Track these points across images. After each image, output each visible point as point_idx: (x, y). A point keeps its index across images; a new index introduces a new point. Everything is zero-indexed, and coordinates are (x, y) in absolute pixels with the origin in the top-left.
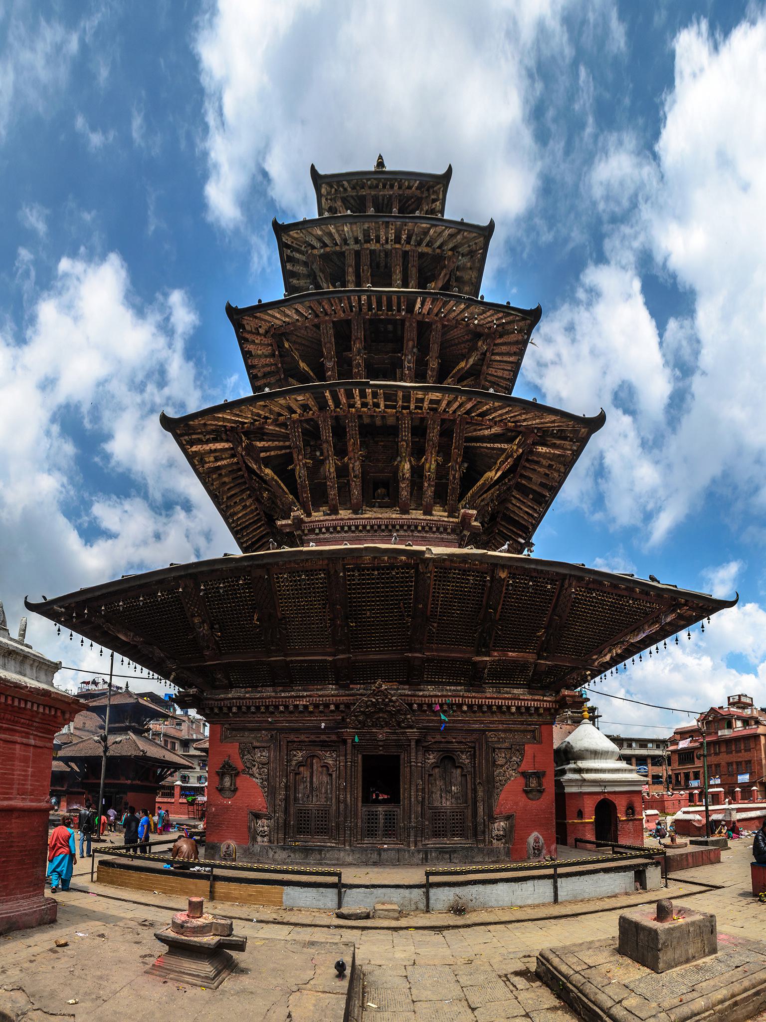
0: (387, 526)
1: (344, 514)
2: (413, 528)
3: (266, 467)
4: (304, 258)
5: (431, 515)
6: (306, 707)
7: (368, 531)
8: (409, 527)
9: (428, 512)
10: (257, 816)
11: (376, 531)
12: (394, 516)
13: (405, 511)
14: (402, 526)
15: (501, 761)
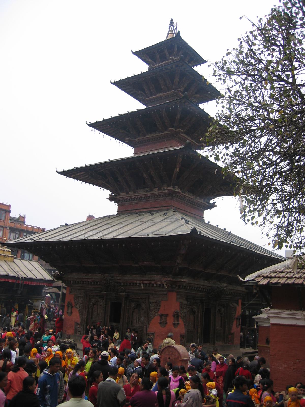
7: (139, 200)
9: (160, 189)
10: (78, 324)
13: (151, 190)
14: (149, 197)
15: (152, 308)
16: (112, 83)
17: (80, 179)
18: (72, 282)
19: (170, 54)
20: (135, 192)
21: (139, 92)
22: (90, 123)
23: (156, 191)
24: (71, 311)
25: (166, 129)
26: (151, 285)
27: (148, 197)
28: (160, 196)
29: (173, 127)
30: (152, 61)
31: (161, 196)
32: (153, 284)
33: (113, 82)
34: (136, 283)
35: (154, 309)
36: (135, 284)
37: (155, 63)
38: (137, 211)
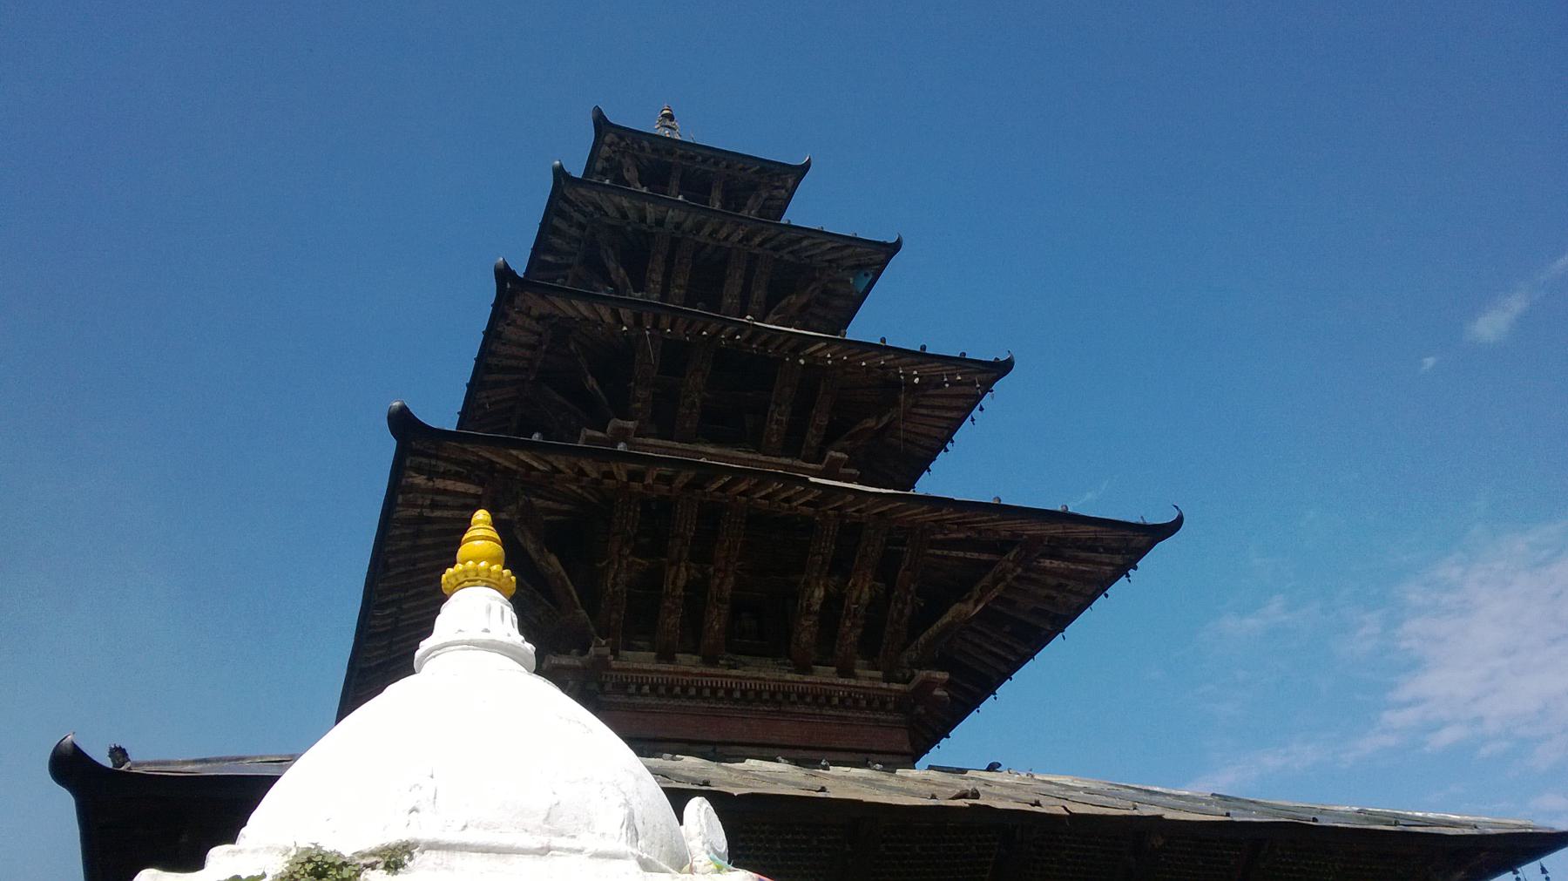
0: (773, 694)
1: (687, 663)
2: (822, 700)
3: (550, 551)
4: (582, 219)
5: (855, 677)
7: (737, 701)
8: (816, 697)
9: (846, 671)
12: (789, 677)
14: (802, 696)
21: (622, 271)
28: (856, 701)
31: (864, 703)
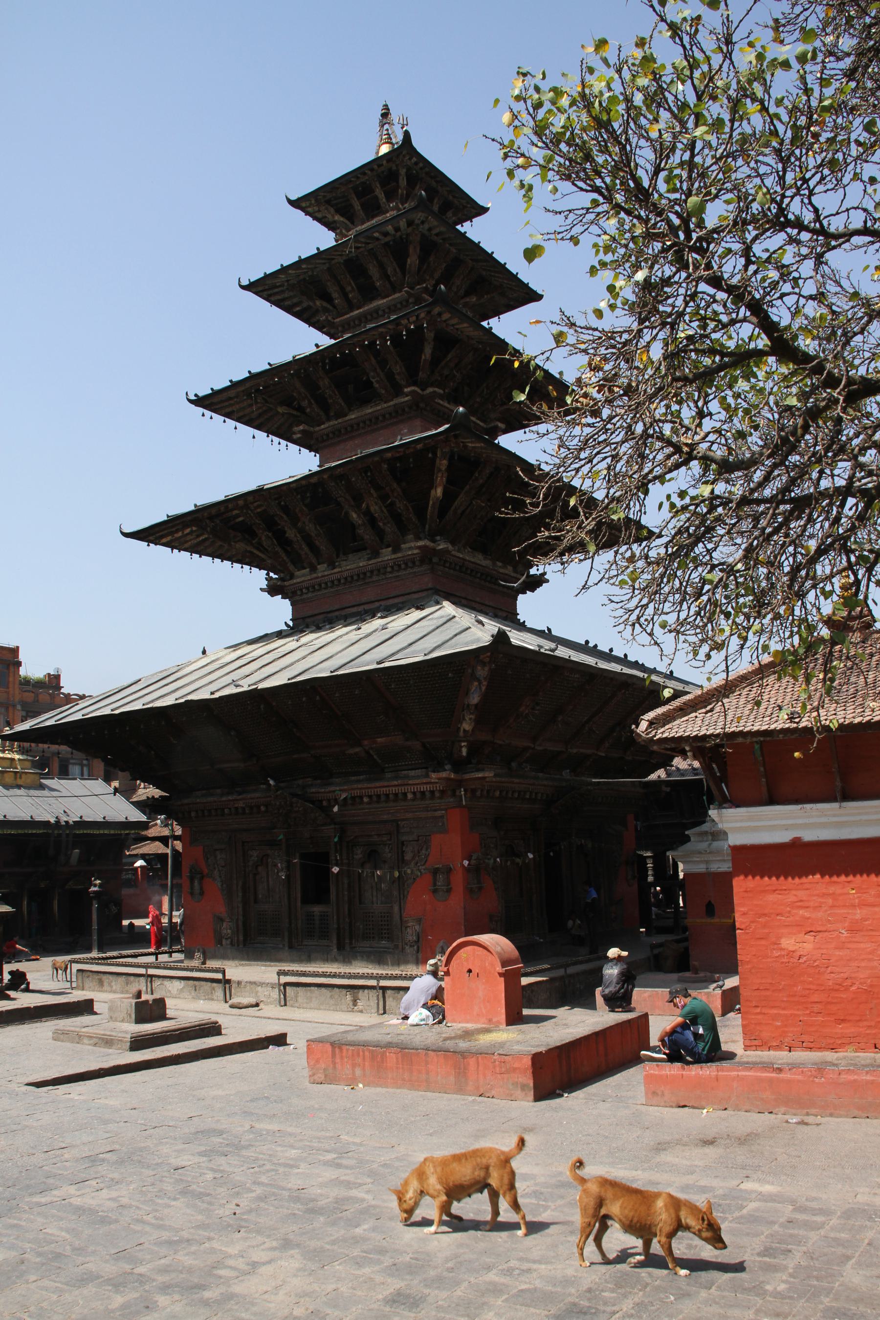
0: (358, 575)
1: (322, 569)
6: (244, 809)
7: (344, 584)
8: (379, 570)
9: (396, 549)
11: (351, 582)
13: (376, 554)
14: (372, 572)
16: (243, 288)
17: (187, 545)
18: (193, 814)
19: (390, 196)
20: (332, 565)
21: (318, 303)
22: (196, 395)
23: (387, 555)
24: (201, 888)
25: (398, 391)
26: (400, 796)
27: (368, 574)
28: (399, 566)
29: (415, 384)
30: (342, 219)
31: (403, 566)
32: (405, 794)
33: (245, 283)
34: (361, 797)
35: (413, 858)
36: (358, 800)
37: (353, 223)
38: (343, 613)
